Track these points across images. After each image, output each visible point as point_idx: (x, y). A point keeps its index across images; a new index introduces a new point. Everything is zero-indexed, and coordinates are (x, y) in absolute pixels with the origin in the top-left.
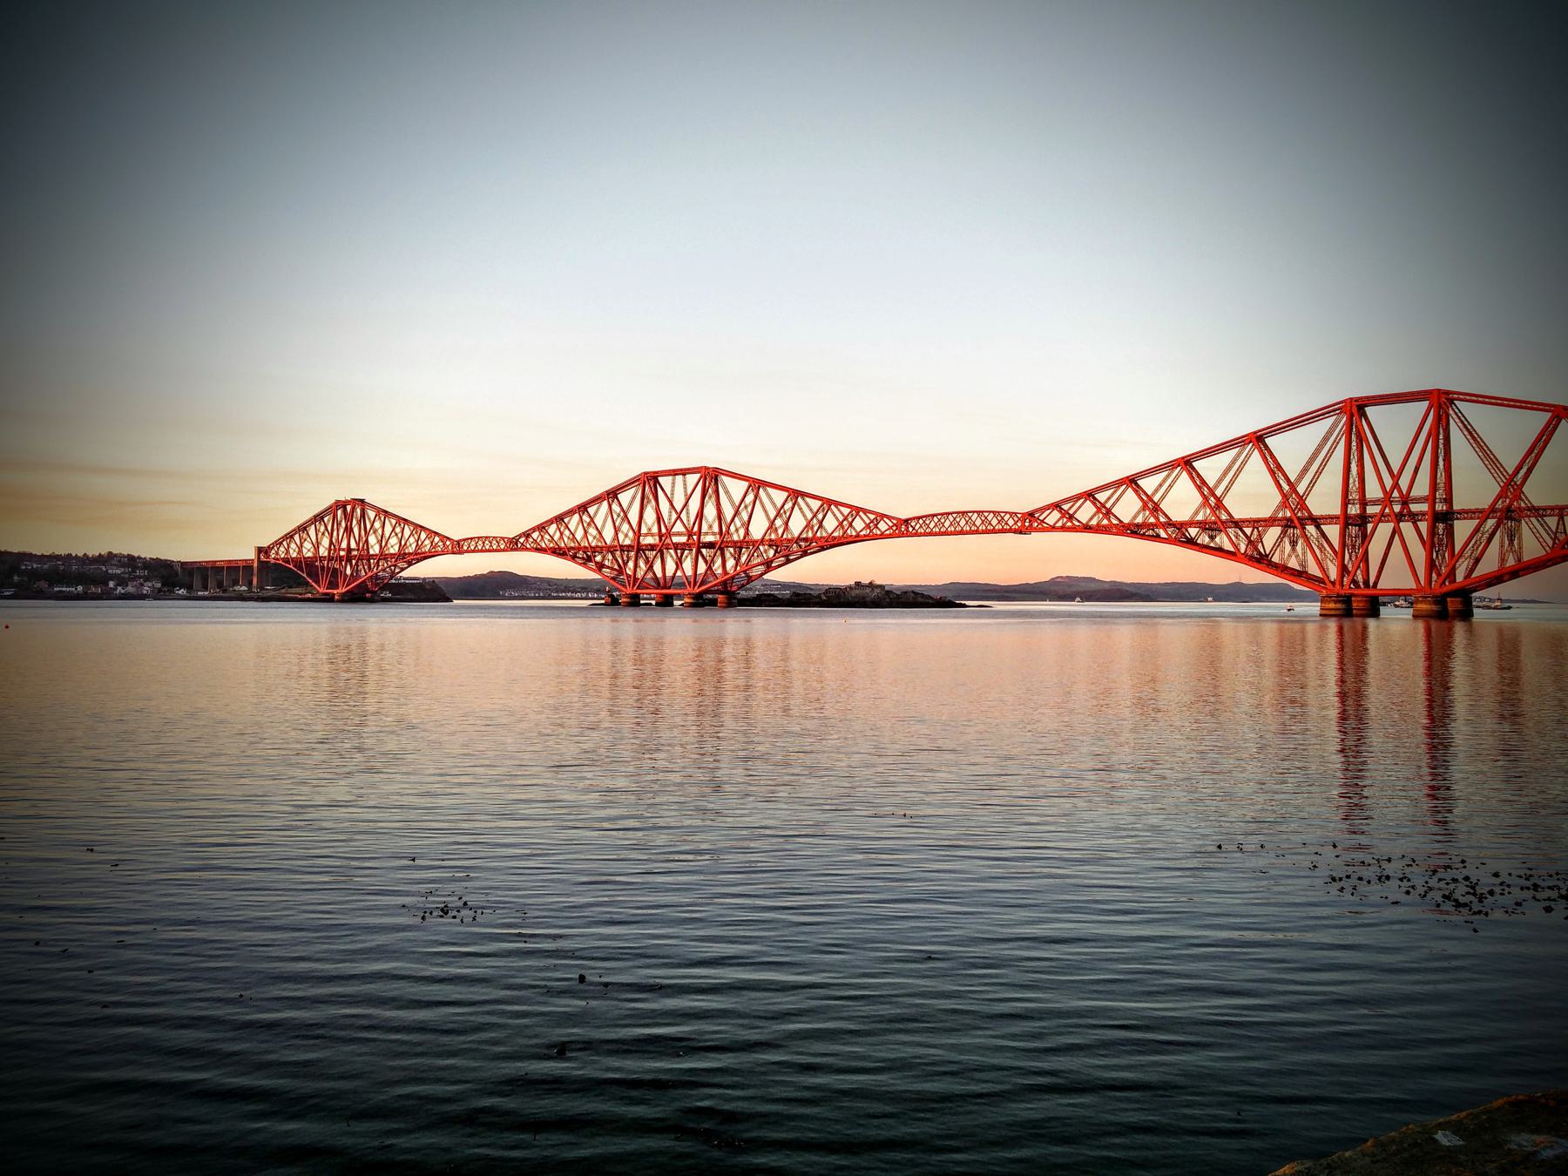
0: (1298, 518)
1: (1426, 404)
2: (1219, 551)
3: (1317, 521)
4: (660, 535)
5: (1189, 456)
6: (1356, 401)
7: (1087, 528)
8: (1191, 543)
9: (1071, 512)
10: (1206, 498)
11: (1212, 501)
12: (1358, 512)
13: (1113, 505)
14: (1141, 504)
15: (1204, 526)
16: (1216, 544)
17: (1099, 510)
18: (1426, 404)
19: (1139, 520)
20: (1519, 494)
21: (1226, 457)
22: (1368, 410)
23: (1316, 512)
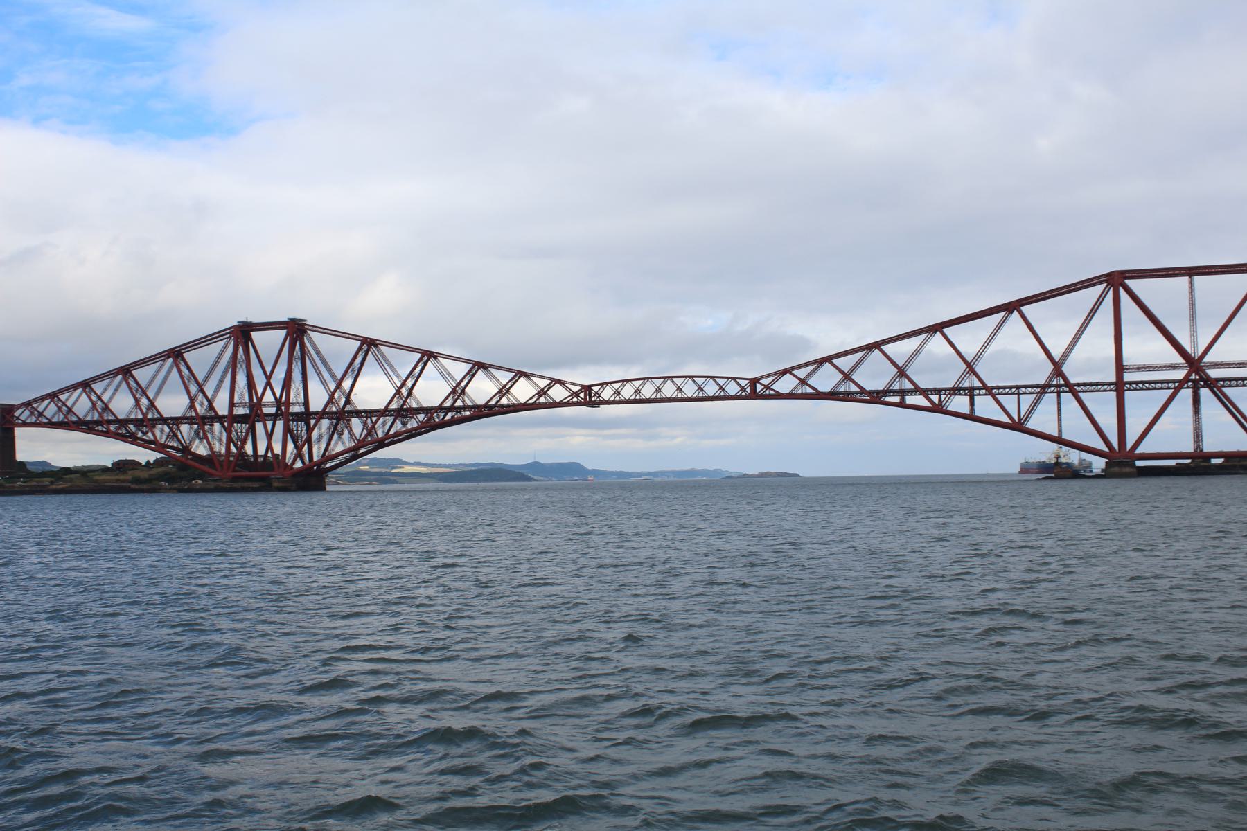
0: (150, 419)
1: (284, 332)
2: (145, 444)
3: (220, 419)
4: (252, 405)
7: (51, 424)
8: (132, 439)
9: (40, 409)
10: (137, 401)
11: (144, 401)
12: (248, 412)
13: (74, 403)
14: (90, 404)
15: (139, 423)
16: (148, 437)
17: (59, 409)
18: (284, 332)
19: (89, 418)
20: (348, 402)
21: (153, 368)
22: (254, 335)
23: (220, 413)
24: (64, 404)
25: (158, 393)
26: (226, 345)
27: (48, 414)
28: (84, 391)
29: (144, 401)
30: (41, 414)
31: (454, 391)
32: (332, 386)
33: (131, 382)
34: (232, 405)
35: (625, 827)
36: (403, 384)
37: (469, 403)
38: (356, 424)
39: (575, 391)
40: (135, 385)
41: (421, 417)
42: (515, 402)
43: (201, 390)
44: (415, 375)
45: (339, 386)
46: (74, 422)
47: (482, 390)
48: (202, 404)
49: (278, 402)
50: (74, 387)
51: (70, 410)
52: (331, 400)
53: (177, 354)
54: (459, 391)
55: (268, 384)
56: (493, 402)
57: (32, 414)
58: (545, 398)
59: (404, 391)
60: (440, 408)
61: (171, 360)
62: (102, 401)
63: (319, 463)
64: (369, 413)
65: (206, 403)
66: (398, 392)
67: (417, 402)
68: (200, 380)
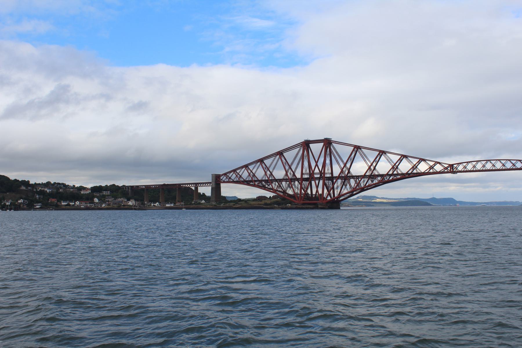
0: (270, 180)
2: (269, 190)
3: (298, 180)
5: (262, 158)
6: (305, 142)
7: (234, 182)
8: (264, 188)
9: (230, 176)
10: (266, 173)
11: (268, 173)
12: (309, 177)
13: (242, 174)
15: (266, 181)
17: (237, 176)
19: (247, 179)
20: (349, 172)
22: (311, 145)
24: (238, 174)
25: (274, 169)
26: (300, 150)
27: (233, 178)
28: (246, 169)
29: (268, 173)
30: (230, 178)
31: (393, 167)
32: (342, 166)
33: (263, 165)
34: (302, 174)
35: (485, 347)
36: (372, 165)
37: (400, 173)
38: (352, 182)
39: (446, 167)
40: (265, 166)
41: (379, 178)
42: (420, 172)
43: (290, 168)
44: (377, 161)
45: (345, 165)
46: (242, 181)
47: (405, 167)
48: (290, 174)
49: (321, 172)
50: (242, 167)
51: (241, 176)
52: (342, 171)
53: (280, 154)
54: (395, 167)
55: (317, 165)
56: (410, 172)
57: (227, 178)
58: (433, 170)
59: (372, 168)
60: (387, 174)
61: (278, 156)
62: (253, 173)
63: (337, 198)
64: (358, 177)
65: (292, 173)
66: (370, 168)
67: (378, 172)
68: (290, 164)
